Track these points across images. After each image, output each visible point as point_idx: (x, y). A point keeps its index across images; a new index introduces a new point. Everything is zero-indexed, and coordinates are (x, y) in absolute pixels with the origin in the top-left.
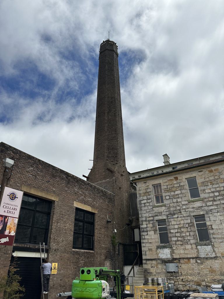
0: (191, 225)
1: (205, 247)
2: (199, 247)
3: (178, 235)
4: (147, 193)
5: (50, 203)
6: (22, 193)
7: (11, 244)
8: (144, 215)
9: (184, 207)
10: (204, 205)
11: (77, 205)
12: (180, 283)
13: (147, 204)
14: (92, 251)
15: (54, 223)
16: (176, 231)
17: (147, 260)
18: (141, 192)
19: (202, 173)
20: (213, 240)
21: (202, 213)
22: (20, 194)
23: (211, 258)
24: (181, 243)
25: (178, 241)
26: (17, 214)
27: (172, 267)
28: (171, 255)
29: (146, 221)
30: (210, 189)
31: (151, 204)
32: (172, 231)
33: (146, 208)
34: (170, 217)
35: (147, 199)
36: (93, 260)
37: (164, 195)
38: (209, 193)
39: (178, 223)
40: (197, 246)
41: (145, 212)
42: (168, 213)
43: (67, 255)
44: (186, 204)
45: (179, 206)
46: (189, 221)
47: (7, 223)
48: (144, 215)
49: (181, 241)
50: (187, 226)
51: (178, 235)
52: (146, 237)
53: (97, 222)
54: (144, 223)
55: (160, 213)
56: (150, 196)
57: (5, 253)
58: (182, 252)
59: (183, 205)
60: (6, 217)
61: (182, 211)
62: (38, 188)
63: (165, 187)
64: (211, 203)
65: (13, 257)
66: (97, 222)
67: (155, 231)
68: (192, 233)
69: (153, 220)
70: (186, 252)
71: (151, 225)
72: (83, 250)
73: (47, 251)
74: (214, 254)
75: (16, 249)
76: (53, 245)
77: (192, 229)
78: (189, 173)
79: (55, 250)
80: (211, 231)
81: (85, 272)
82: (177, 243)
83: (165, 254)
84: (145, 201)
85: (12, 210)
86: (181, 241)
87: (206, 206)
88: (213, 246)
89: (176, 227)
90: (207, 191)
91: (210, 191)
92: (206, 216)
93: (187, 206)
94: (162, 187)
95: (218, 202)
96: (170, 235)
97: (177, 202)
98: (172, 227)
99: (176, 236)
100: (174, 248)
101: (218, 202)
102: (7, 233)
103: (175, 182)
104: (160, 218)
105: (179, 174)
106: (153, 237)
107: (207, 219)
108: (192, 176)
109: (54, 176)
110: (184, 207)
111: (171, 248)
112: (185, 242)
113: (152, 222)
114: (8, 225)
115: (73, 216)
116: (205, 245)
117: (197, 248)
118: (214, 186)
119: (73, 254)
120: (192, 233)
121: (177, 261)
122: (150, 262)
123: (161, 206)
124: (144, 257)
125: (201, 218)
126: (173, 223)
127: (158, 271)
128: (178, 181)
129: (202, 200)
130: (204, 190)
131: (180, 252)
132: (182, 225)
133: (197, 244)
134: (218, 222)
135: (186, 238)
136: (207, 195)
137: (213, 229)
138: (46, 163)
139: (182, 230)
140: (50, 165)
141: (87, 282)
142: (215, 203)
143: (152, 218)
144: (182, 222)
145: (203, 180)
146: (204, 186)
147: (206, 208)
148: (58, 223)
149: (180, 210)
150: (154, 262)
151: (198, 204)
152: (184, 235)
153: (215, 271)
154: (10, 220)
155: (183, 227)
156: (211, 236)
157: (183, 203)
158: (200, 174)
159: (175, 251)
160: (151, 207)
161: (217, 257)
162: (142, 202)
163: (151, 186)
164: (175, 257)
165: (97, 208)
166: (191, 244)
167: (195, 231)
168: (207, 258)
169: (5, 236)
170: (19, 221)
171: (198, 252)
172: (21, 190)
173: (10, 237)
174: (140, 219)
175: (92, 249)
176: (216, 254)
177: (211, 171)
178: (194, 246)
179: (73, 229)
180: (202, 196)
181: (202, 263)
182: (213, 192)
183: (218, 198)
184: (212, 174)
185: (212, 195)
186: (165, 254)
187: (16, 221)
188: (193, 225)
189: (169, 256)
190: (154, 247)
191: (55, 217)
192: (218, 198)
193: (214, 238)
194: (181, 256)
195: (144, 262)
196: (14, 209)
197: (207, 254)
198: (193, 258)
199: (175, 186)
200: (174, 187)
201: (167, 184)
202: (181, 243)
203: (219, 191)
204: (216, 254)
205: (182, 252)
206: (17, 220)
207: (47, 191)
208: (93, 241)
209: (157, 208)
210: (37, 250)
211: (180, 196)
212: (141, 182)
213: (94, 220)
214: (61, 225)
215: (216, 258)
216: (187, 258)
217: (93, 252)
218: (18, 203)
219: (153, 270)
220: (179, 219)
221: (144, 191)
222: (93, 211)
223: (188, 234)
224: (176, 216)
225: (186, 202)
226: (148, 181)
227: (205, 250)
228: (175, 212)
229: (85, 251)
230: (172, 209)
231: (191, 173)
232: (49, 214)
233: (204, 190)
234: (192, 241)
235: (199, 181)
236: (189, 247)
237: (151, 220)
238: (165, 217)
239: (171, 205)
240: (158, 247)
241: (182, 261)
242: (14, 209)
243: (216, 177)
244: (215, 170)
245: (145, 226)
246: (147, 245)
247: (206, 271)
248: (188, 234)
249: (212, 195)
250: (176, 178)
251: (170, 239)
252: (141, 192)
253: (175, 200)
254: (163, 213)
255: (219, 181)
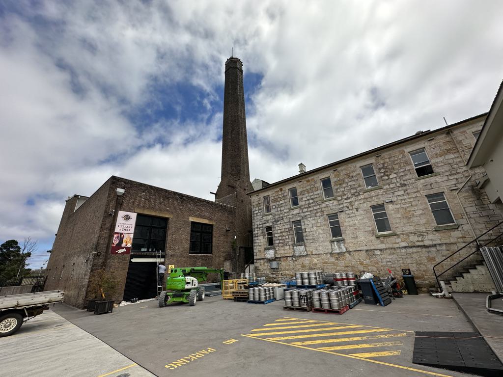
0: (290, 229)
1: (300, 247)
2: (295, 247)
3: (280, 238)
4: (259, 205)
5: (167, 219)
6: (136, 214)
7: (129, 253)
8: (256, 223)
9: (286, 215)
10: (301, 212)
11: (191, 219)
12: (280, 276)
13: (259, 214)
14: (210, 255)
15: (169, 235)
16: (279, 235)
17: (257, 259)
18: (255, 204)
19: (301, 183)
20: (306, 241)
21: (299, 219)
22: (134, 216)
23: (303, 256)
24: (282, 245)
25: (280, 243)
26: (132, 231)
27: (274, 265)
28: (275, 255)
29: (257, 228)
30: (306, 197)
31: (261, 214)
32: (276, 235)
33: (258, 217)
34: (275, 223)
35: (259, 210)
36: (211, 262)
37: (271, 205)
38: (305, 201)
39: (280, 228)
40: (293, 247)
41: (256, 220)
42: (273, 220)
43: (183, 259)
44: (288, 212)
45: (282, 214)
46: (289, 226)
47: (123, 238)
48: (256, 223)
49: (282, 243)
50: (287, 230)
51: (280, 238)
52: (257, 241)
53: (215, 231)
54: (256, 230)
55: (268, 221)
56: (261, 207)
57: (123, 260)
58: (282, 252)
59: (285, 213)
60: (122, 234)
61: (284, 218)
62: (152, 209)
63: (273, 198)
64: (306, 210)
65: (131, 262)
66: (215, 231)
67: (264, 236)
68: (290, 237)
69: (262, 227)
70: (285, 252)
71: (261, 231)
72: (200, 255)
73: (163, 257)
74: (306, 252)
75: (132, 257)
76: (169, 252)
77: (291, 233)
78: (290, 184)
79: (171, 256)
80: (304, 234)
81: (174, 272)
82: (279, 245)
83: (270, 254)
84: (257, 212)
85: (127, 228)
86: (282, 243)
87: (303, 212)
88: (305, 246)
89: (279, 231)
90: (304, 199)
91: (306, 199)
92: (302, 221)
93: (288, 214)
94: (271, 198)
95: (312, 209)
96: (274, 239)
97: (281, 211)
98: (276, 232)
99: (278, 240)
100: (277, 249)
101: (312, 209)
102: (124, 245)
103: (280, 193)
104: (268, 225)
105: (283, 185)
106: (262, 241)
107: (302, 224)
108: (294, 186)
109: (166, 198)
110: (286, 215)
111: (275, 249)
112: (285, 244)
113: (261, 229)
114: (124, 239)
115: (189, 229)
116: (300, 245)
117: (293, 249)
118: (310, 194)
119: (190, 258)
120: (290, 237)
121: (278, 259)
122: (259, 261)
123: (269, 215)
124: (255, 257)
125: (298, 223)
126: (277, 228)
127: (265, 268)
128: (283, 192)
129: (300, 208)
130: (302, 198)
131: (281, 252)
132: (283, 230)
133: (294, 245)
134: (310, 226)
135: (286, 241)
136: (303, 203)
137: (306, 232)
138: (158, 188)
139: (284, 234)
140: (162, 189)
141: (174, 278)
142: (309, 209)
143: (261, 226)
144: (284, 227)
145: (301, 190)
146: (302, 195)
147: (302, 214)
148: (173, 235)
149: (282, 217)
150: (262, 261)
151: (296, 211)
152: (284, 238)
153: (305, 266)
154: (126, 236)
155: (284, 232)
156: (305, 238)
157: (285, 211)
158: (299, 184)
159: (277, 252)
160: (262, 216)
161: (308, 255)
162: (255, 212)
163: (262, 198)
164: (277, 256)
165: (215, 221)
166: (289, 245)
167: (293, 234)
168: (300, 256)
169: (123, 248)
170: (134, 236)
171: (294, 251)
172: (134, 212)
173: (127, 248)
174: (253, 227)
175: (211, 253)
176: (307, 252)
177: (308, 181)
178: (291, 247)
179: (189, 239)
180: (300, 203)
181: (296, 261)
182: (308, 200)
183: (312, 205)
184: (309, 183)
185: (307, 202)
186: (270, 254)
187: (132, 236)
188: (292, 230)
189: (273, 256)
190: (262, 249)
191: (170, 231)
192: (312, 205)
193: (307, 239)
194: (282, 255)
195: (255, 261)
196: (129, 227)
197: (301, 253)
198: (290, 257)
199: (280, 196)
200: (279, 197)
201: (274, 195)
202: (282, 245)
203: (313, 199)
204: (307, 252)
205: (282, 252)
206: (132, 235)
207: (161, 210)
208: (212, 247)
209: (266, 217)
210: (154, 257)
211: (283, 205)
212: (254, 195)
213: (212, 230)
214: (176, 236)
215: (307, 256)
216: (286, 257)
217: (211, 255)
218: (133, 222)
219: (261, 268)
220: (282, 225)
221: (257, 203)
222: (211, 223)
223: (287, 237)
224: (279, 223)
225: (288, 210)
226: (260, 194)
227: (299, 250)
228: (279, 219)
229: (202, 255)
230: (276, 217)
231: (292, 184)
232: (165, 229)
233: (302, 198)
234: (290, 243)
235: (299, 191)
236: (287, 247)
237: (261, 227)
238: (271, 224)
239: (276, 213)
240: (266, 249)
241: (282, 259)
242: (129, 227)
243: (312, 186)
244: (312, 180)
245: (256, 232)
246: (258, 247)
247: (299, 267)
248: (287, 237)
249: (307, 202)
250: (281, 190)
251: (274, 242)
252: (255, 204)
253: (279, 209)
254: (270, 221)
255: (314, 189)
